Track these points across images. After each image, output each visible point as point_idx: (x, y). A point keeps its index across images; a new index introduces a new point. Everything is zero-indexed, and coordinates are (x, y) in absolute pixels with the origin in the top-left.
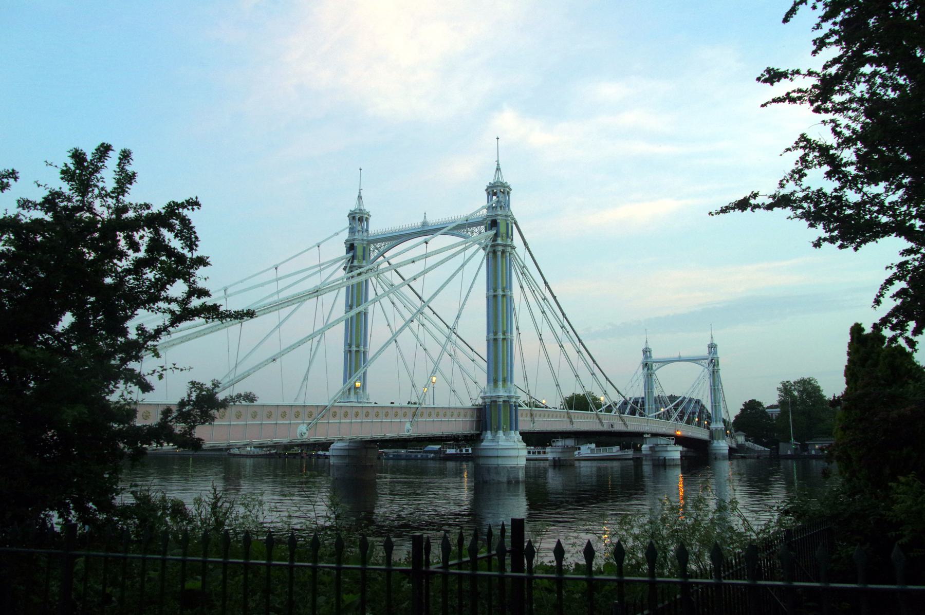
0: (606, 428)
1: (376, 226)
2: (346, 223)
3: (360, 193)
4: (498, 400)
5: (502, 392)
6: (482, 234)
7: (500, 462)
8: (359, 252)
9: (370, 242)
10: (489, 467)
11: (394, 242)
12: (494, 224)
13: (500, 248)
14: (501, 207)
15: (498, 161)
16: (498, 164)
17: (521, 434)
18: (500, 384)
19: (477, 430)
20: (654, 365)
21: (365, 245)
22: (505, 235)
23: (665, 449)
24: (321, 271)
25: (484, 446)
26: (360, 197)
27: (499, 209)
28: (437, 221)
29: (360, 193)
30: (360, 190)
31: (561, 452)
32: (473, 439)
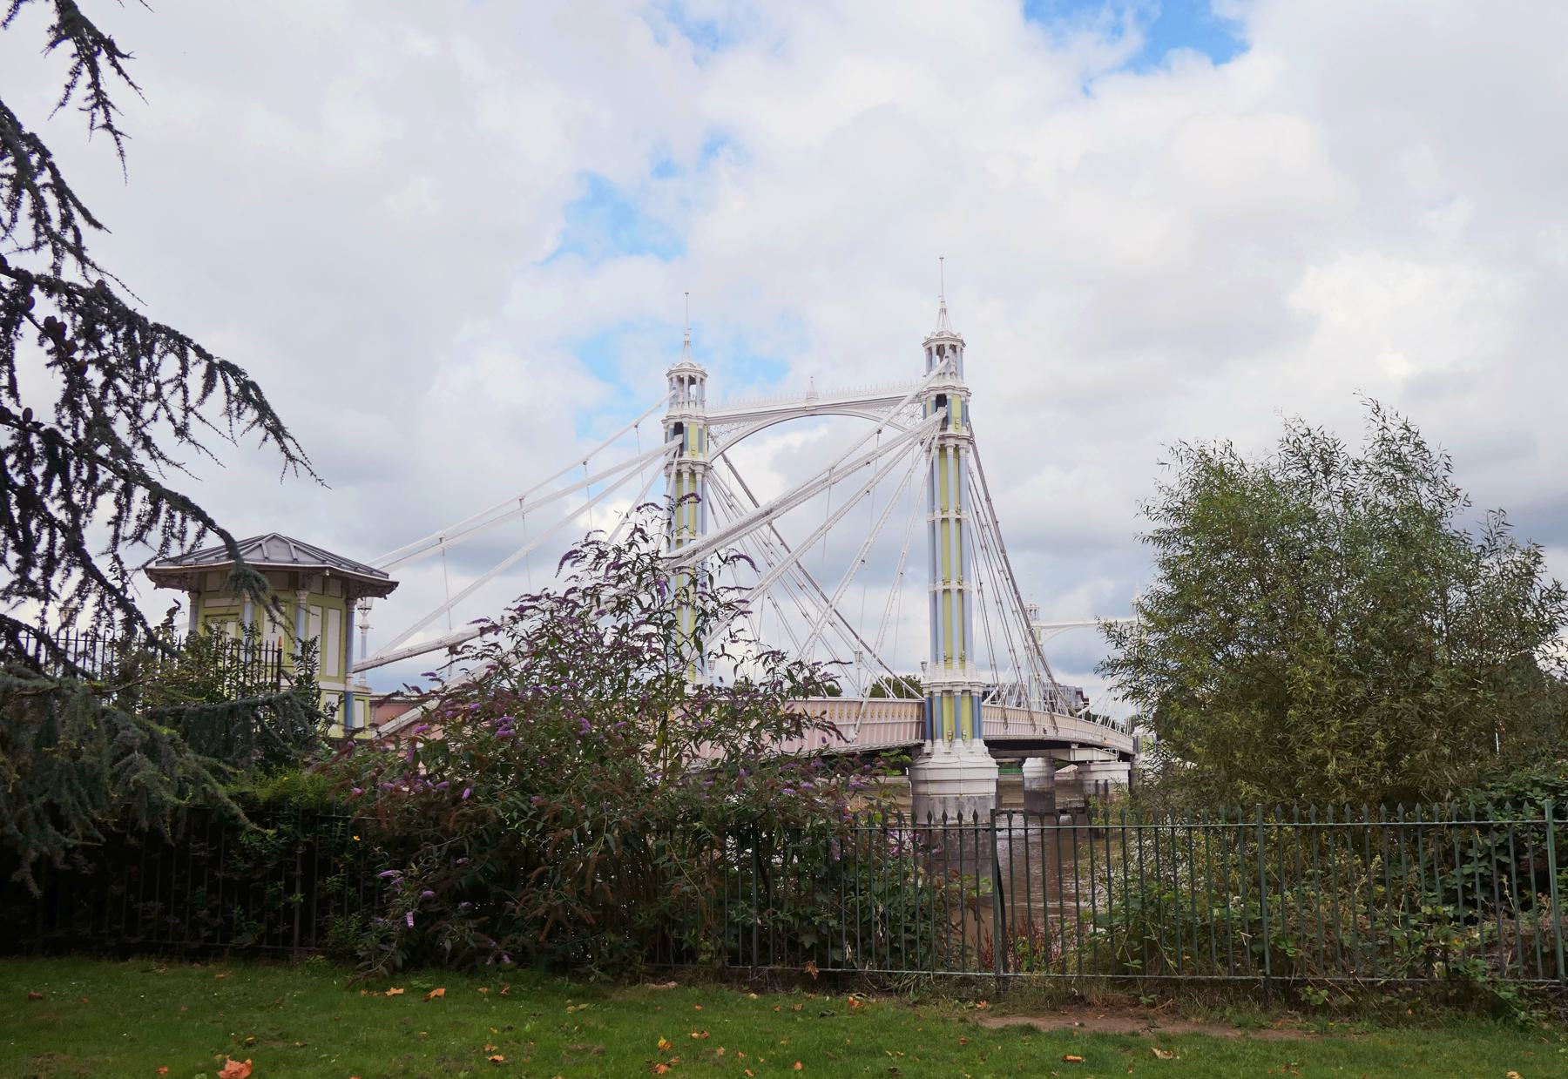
0: (1039, 735)
10: (945, 798)
20: (1043, 632)
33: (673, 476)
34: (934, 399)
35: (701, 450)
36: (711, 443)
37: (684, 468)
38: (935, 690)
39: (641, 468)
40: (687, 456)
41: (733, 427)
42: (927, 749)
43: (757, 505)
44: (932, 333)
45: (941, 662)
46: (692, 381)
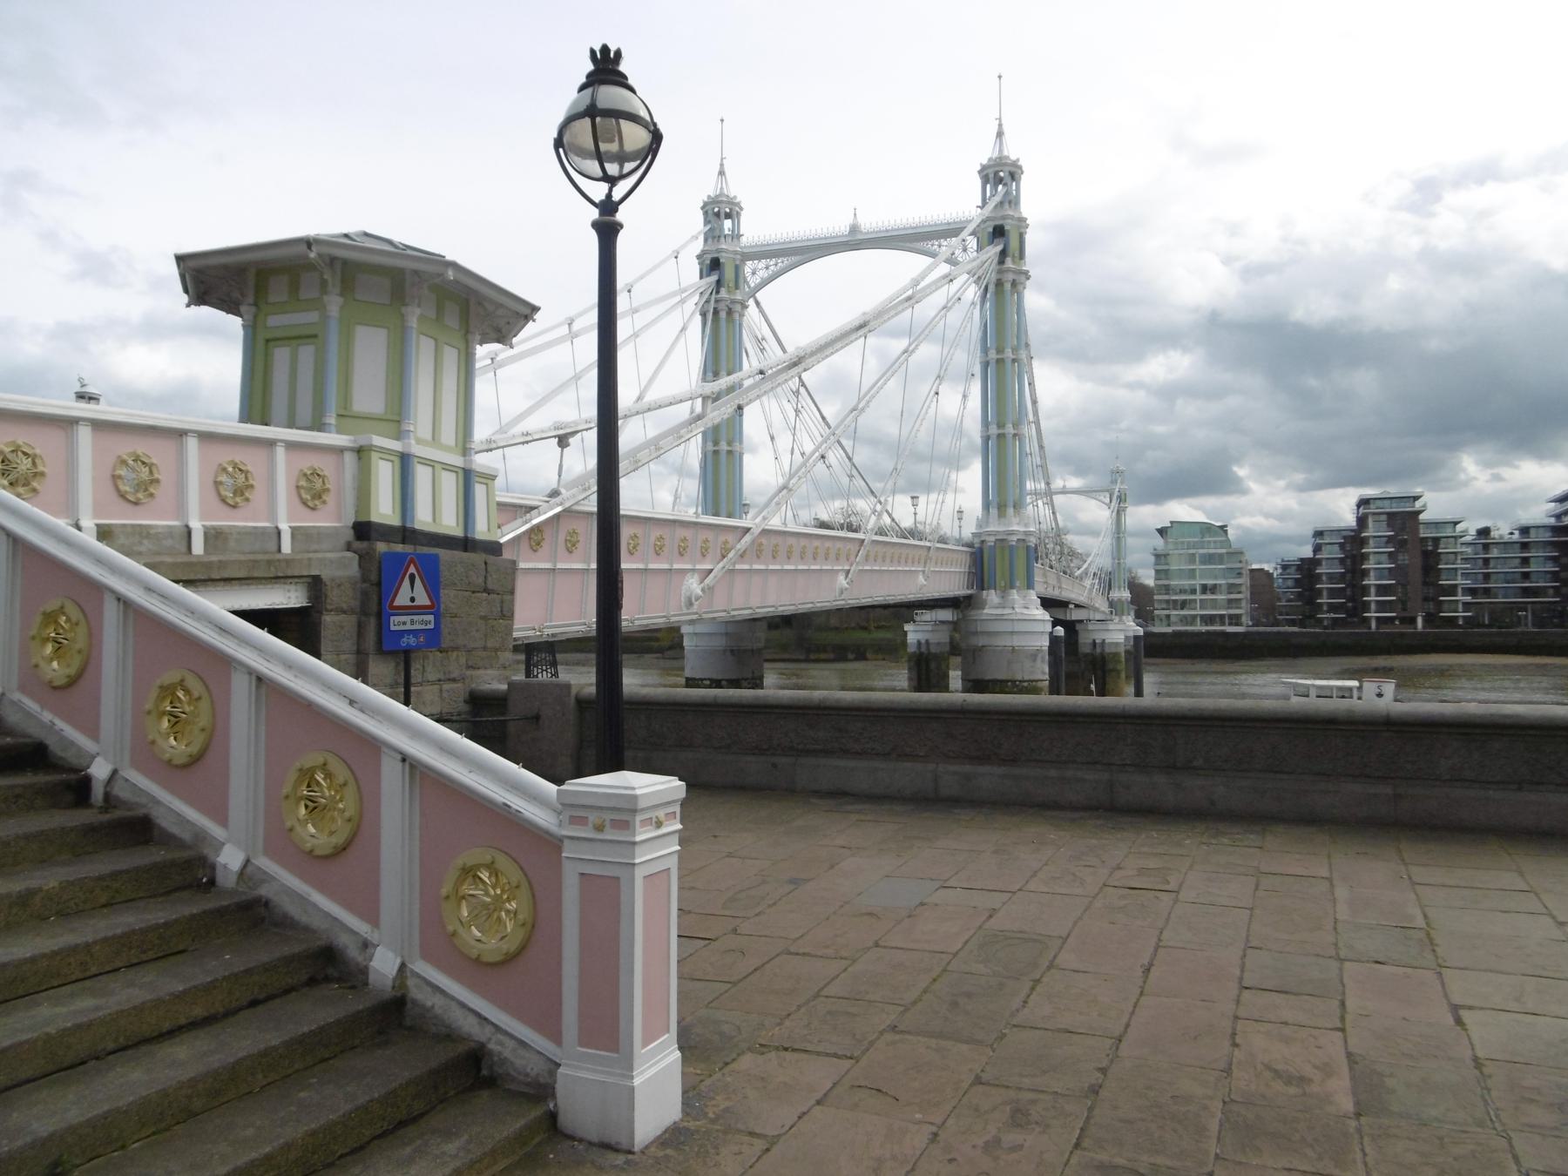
1: (754, 229)
2: (697, 223)
3: (722, 165)
4: (1027, 538)
5: (1015, 526)
6: (970, 251)
7: (1017, 642)
8: (729, 273)
11: (794, 259)
12: (999, 232)
13: (1010, 277)
14: (1010, 202)
15: (1000, 119)
16: (1000, 125)
18: (1011, 511)
19: (970, 586)
21: (738, 263)
22: (1017, 254)
23: (1104, 627)
25: (987, 614)
26: (722, 173)
27: (1006, 206)
28: (773, 236)
29: (722, 165)
30: (722, 159)
31: (932, 631)
33: (710, 317)
34: (991, 230)
35: (737, 287)
37: (722, 306)
38: (987, 538)
39: (683, 301)
40: (723, 293)
41: (772, 263)
43: (784, 351)
44: (990, 159)
46: (728, 216)
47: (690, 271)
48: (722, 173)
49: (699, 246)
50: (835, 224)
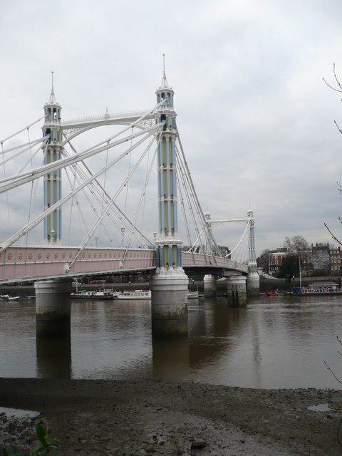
0: (209, 265)
6: (155, 124)
8: (55, 136)
9: (62, 128)
12: (163, 117)
13: (169, 136)
17: (184, 268)
18: (170, 233)
24: (31, 147)
26: (53, 94)
32: (149, 274)
36: (63, 137)
42: (157, 271)
45: (163, 233)
46: (55, 110)
47: (38, 134)
48: (53, 94)
49: (42, 123)
50: (98, 114)
